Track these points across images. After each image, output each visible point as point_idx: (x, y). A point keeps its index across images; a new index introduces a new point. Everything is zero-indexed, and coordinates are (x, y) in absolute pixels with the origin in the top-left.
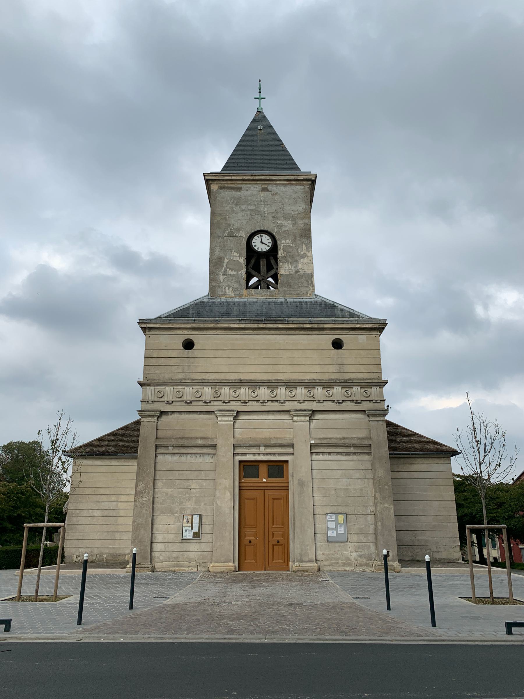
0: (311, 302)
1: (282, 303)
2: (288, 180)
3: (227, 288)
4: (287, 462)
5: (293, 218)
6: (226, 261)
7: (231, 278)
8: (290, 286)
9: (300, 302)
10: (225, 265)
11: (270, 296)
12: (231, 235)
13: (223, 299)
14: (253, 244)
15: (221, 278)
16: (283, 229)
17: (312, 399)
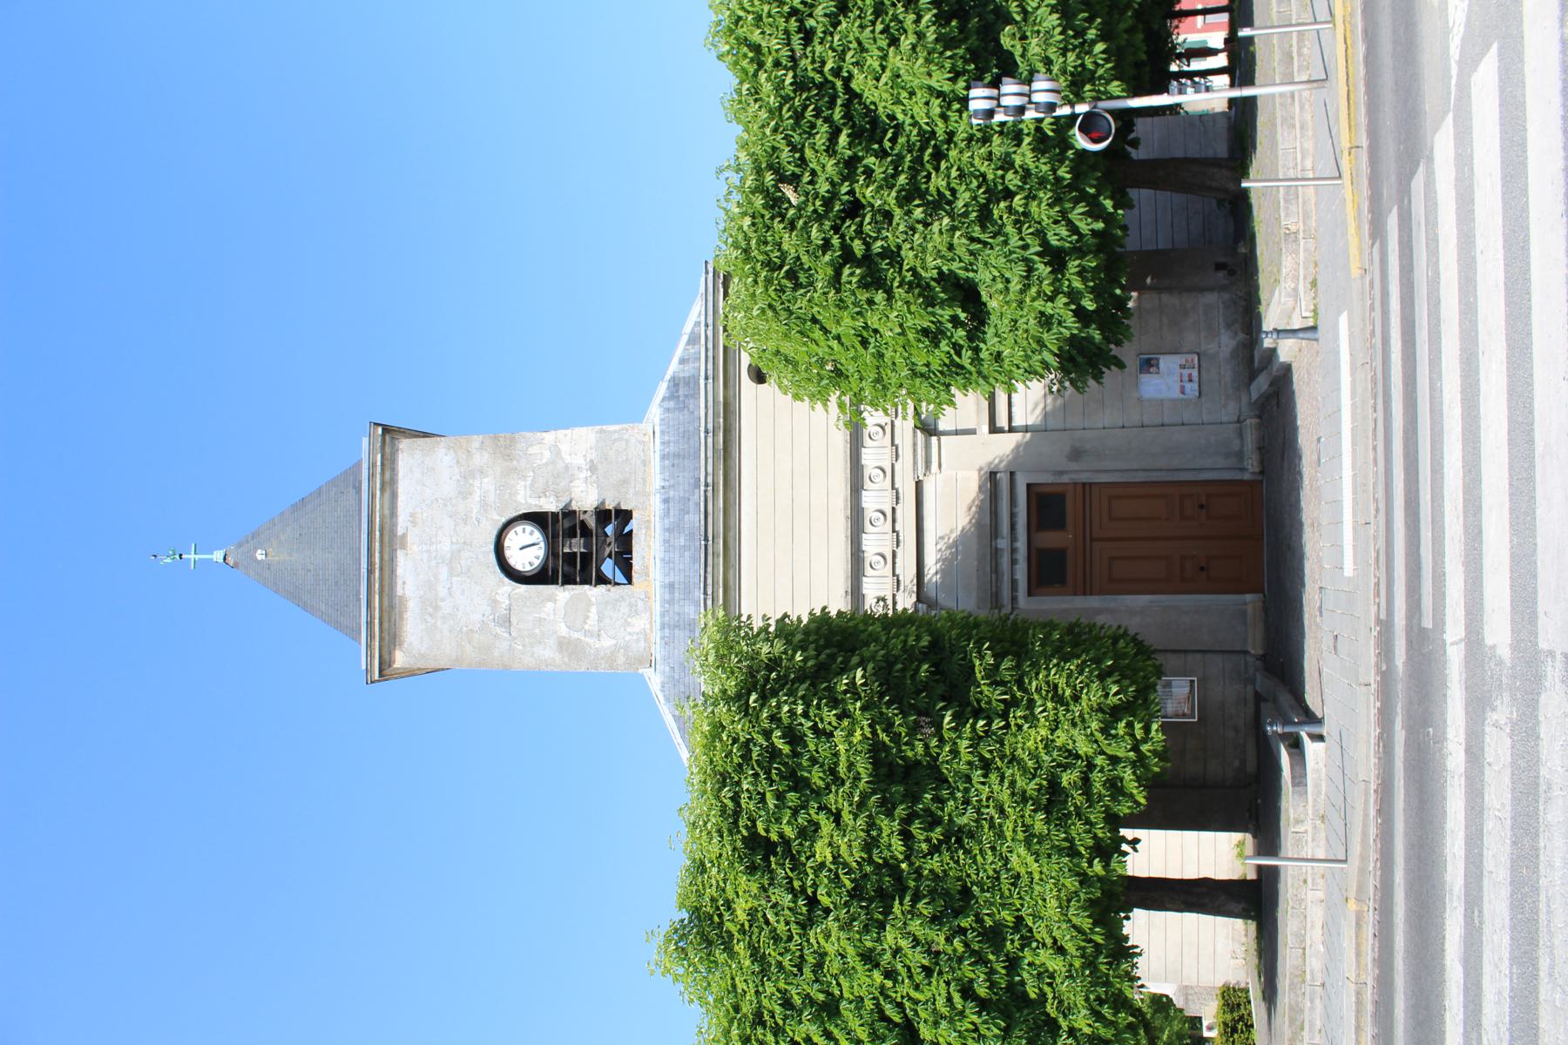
0: (663, 432)
1: (666, 501)
2: (382, 490)
3: (629, 629)
4: (1029, 486)
5: (468, 475)
6: (563, 630)
7: (607, 621)
8: (625, 482)
9: (663, 457)
10: (576, 635)
11: (648, 528)
12: (507, 621)
13: (656, 636)
14: (528, 568)
15: (607, 643)
16: (492, 498)
17: (888, 429)
